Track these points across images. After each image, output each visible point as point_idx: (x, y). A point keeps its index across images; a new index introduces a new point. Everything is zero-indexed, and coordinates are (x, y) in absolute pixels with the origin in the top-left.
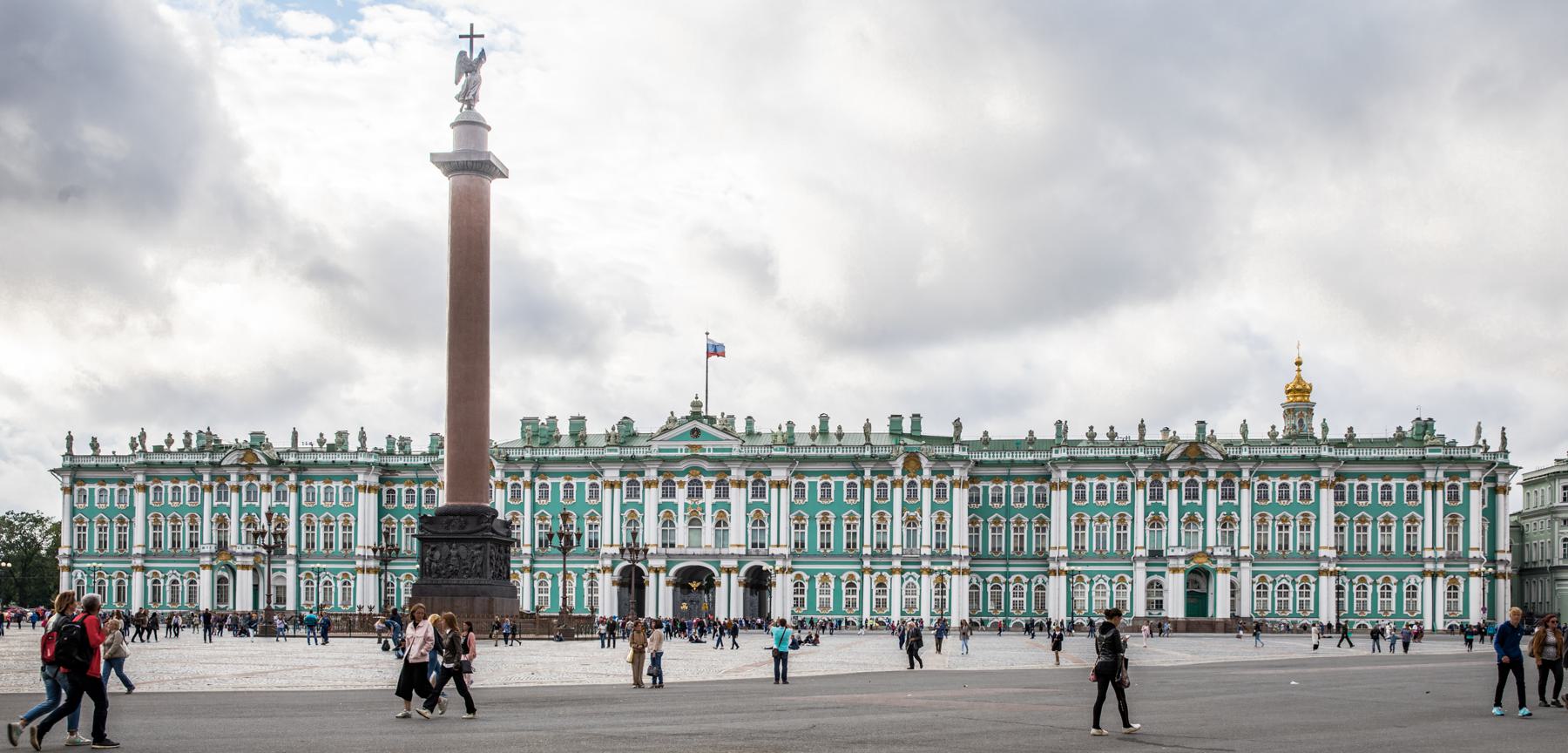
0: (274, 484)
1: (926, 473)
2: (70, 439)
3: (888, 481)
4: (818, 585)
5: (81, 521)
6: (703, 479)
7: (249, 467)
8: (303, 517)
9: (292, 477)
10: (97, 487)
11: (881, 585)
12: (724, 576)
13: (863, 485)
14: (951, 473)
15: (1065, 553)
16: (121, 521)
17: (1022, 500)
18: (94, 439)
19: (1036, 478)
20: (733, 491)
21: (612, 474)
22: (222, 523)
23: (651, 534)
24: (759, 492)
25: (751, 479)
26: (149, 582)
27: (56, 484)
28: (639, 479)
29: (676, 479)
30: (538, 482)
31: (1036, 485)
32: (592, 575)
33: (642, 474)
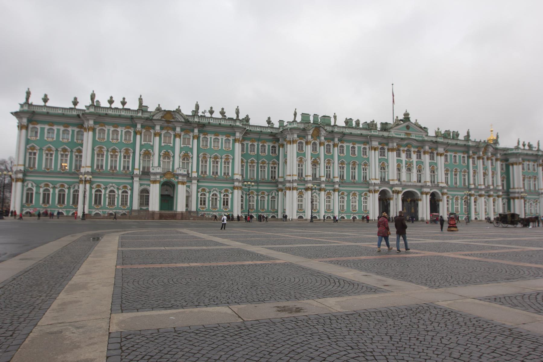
0: (183, 134)
2: (28, 94)
3: (476, 157)
5: (33, 148)
6: (412, 149)
7: (168, 122)
8: (201, 154)
9: (196, 131)
10: (47, 127)
11: (475, 202)
12: (424, 196)
13: (469, 157)
15: (523, 190)
16: (65, 150)
18: (46, 96)
19: (501, 161)
21: (375, 144)
22: (147, 155)
23: (392, 174)
25: (430, 151)
26: (94, 191)
27: (15, 121)
28: (386, 147)
29: (402, 149)
30: (340, 144)
32: (366, 194)
33: (387, 144)
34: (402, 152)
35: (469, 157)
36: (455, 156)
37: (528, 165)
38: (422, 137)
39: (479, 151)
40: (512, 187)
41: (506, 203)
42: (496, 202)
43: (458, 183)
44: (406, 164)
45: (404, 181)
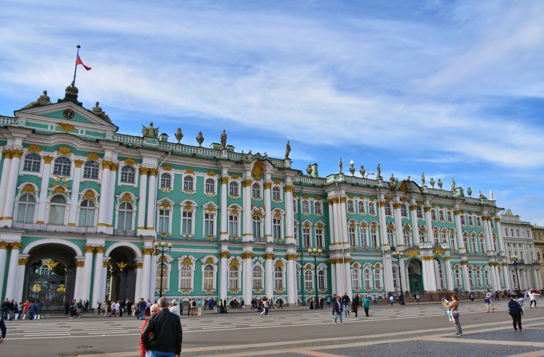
1: (268, 177)
3: (239, 181)
4: (180, 268)
6: (73, 157)
11: (234, 267)
12: (89, 255)
13: (221, 181)
14: (284, 180)
15: (348, 246)
17: (307, 210)
19: (316, 196)
20: (105, 174)
24: (128, 176)
25: (122, 164)
29: (42, 154)
31: (315, 201)
34: (43, 161)
35: (221, 181)
36: (189, 178)
37: (361, 203)
38: (104, 135)
39: (245, 171)
40: (332, 242)
41: (326, 272)
42: (284, 270)
43: (193, 232)
44: (51, 186)
45: (38, 222)
